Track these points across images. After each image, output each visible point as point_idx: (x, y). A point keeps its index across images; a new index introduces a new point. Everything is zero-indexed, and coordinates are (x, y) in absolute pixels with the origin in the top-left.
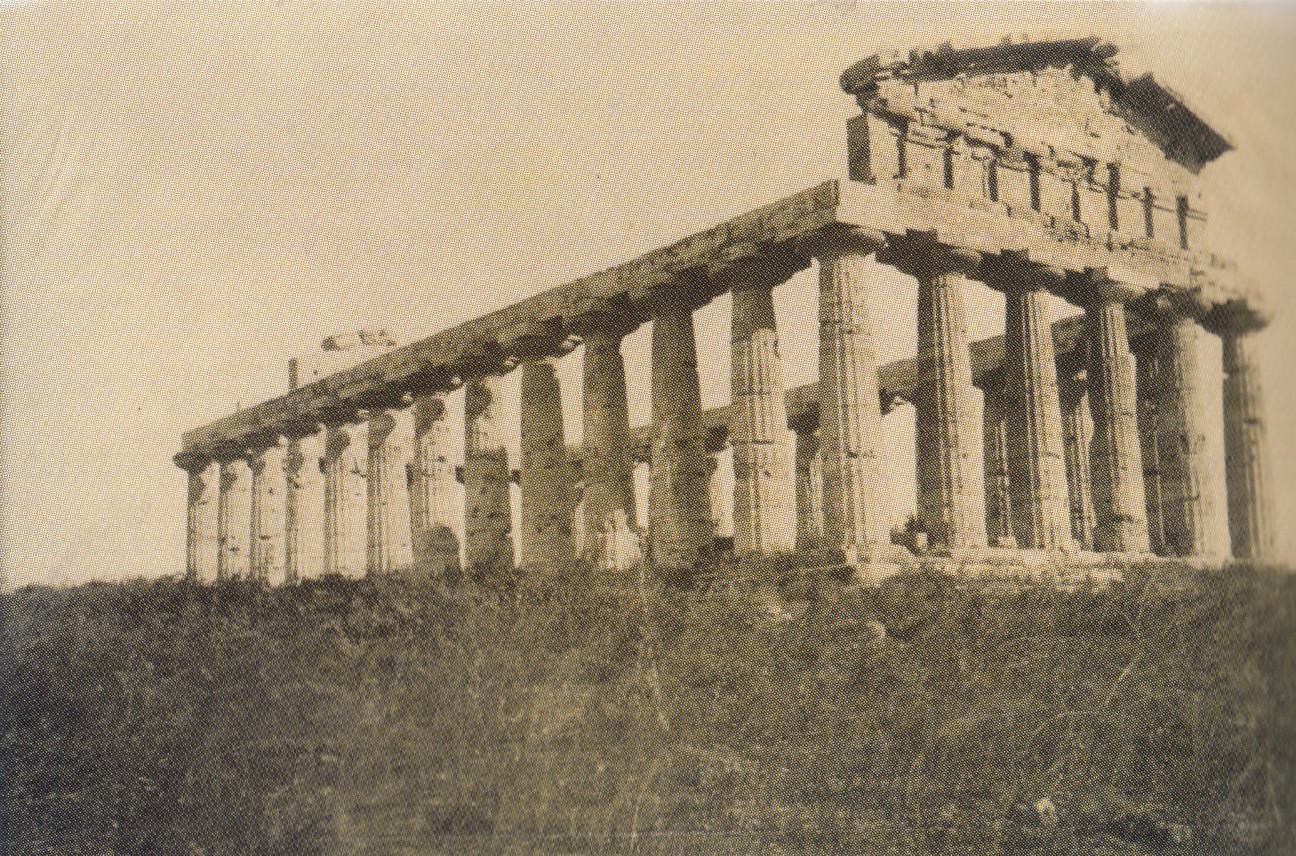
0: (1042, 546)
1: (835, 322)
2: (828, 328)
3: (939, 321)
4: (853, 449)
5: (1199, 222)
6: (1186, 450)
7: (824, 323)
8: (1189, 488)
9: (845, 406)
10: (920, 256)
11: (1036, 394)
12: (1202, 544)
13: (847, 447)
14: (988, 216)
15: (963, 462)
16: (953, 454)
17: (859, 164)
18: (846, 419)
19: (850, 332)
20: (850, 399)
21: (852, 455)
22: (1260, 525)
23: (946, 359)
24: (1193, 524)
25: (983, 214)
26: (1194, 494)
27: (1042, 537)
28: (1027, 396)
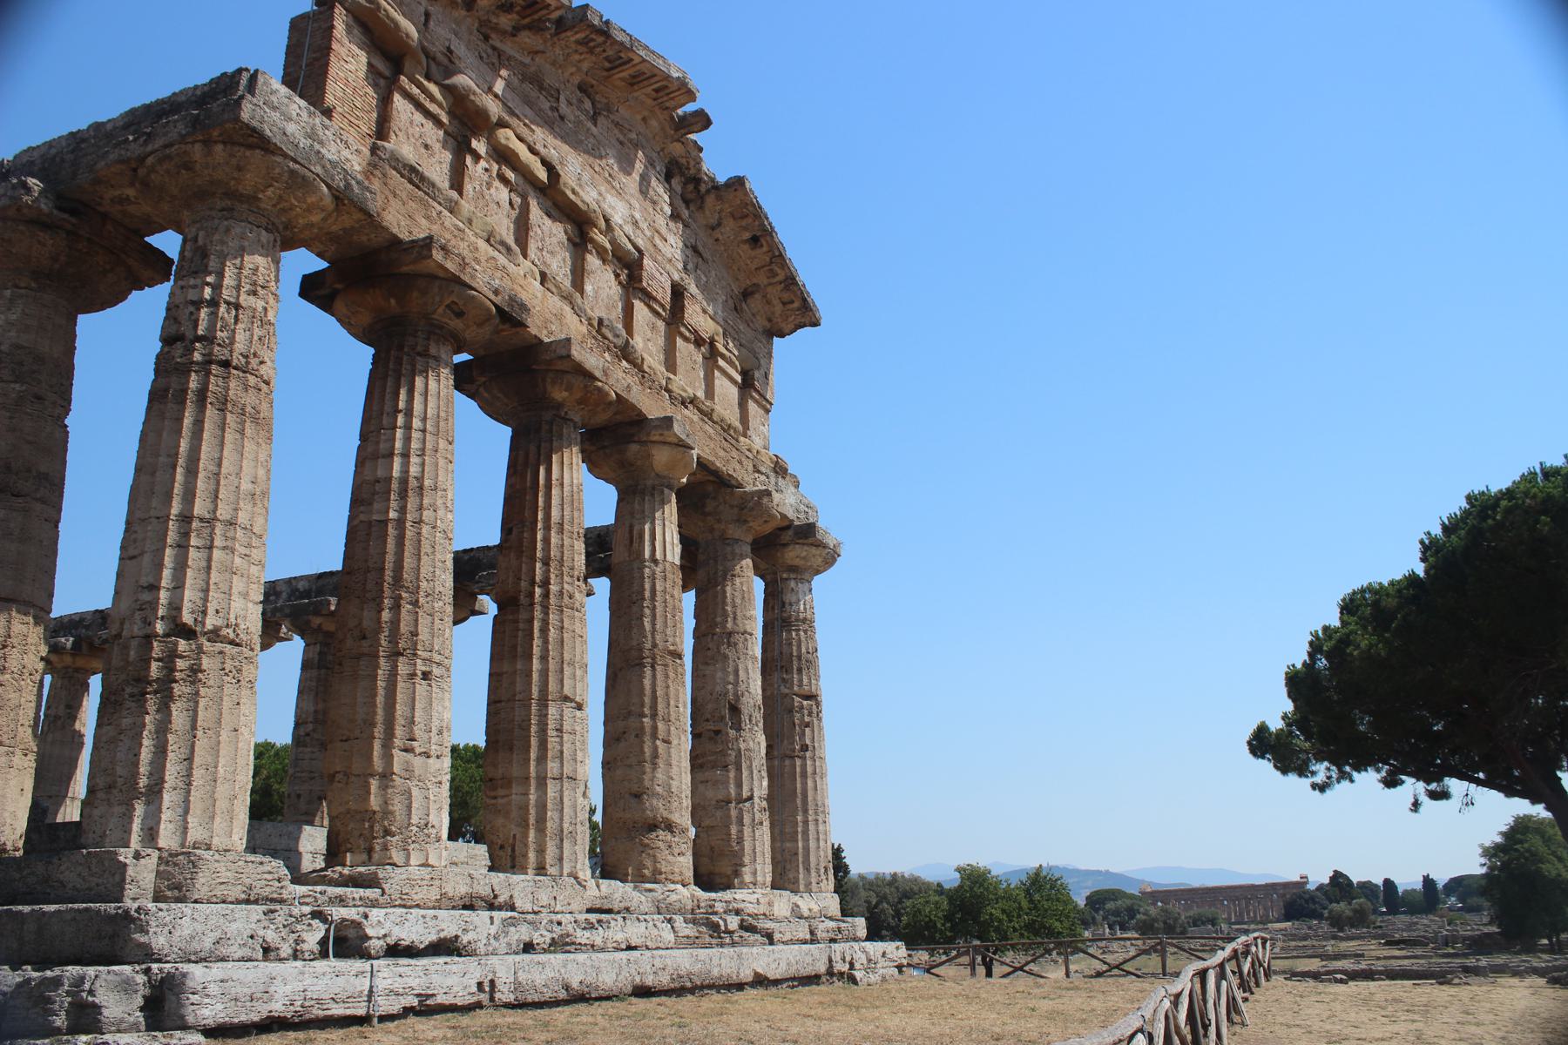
0: (541, 869)
1: (199, 339)
2: (178, 349)
3: (409, 413)
4: (187, 618)
5: (761, 412)
6: (739, 729)
7: (168, 340)
8: (739, 785)
9: (186, 518)
10: (387, 292)
11: (554, 588)
12: (755, 873)
13: (175, 607)
14: (511, 268)
15: (421, 687)
16: (403, 668)
17: (306, 69)
18: (182, 547)
19: (226, 364)
20: (200, 508)
21: (188, 633)
22: (812, 844)
23: (413, 483)
24: (740, 840)
25: (502, 260)
26: (745, 794)
27: (541, 851)
28: (538, 591)
